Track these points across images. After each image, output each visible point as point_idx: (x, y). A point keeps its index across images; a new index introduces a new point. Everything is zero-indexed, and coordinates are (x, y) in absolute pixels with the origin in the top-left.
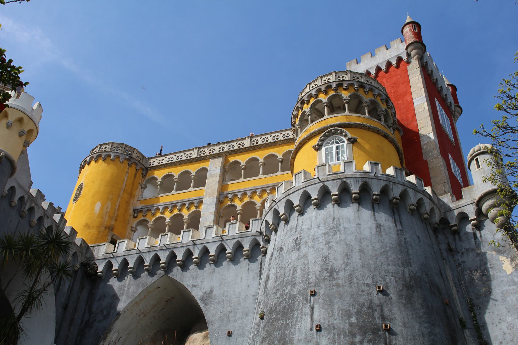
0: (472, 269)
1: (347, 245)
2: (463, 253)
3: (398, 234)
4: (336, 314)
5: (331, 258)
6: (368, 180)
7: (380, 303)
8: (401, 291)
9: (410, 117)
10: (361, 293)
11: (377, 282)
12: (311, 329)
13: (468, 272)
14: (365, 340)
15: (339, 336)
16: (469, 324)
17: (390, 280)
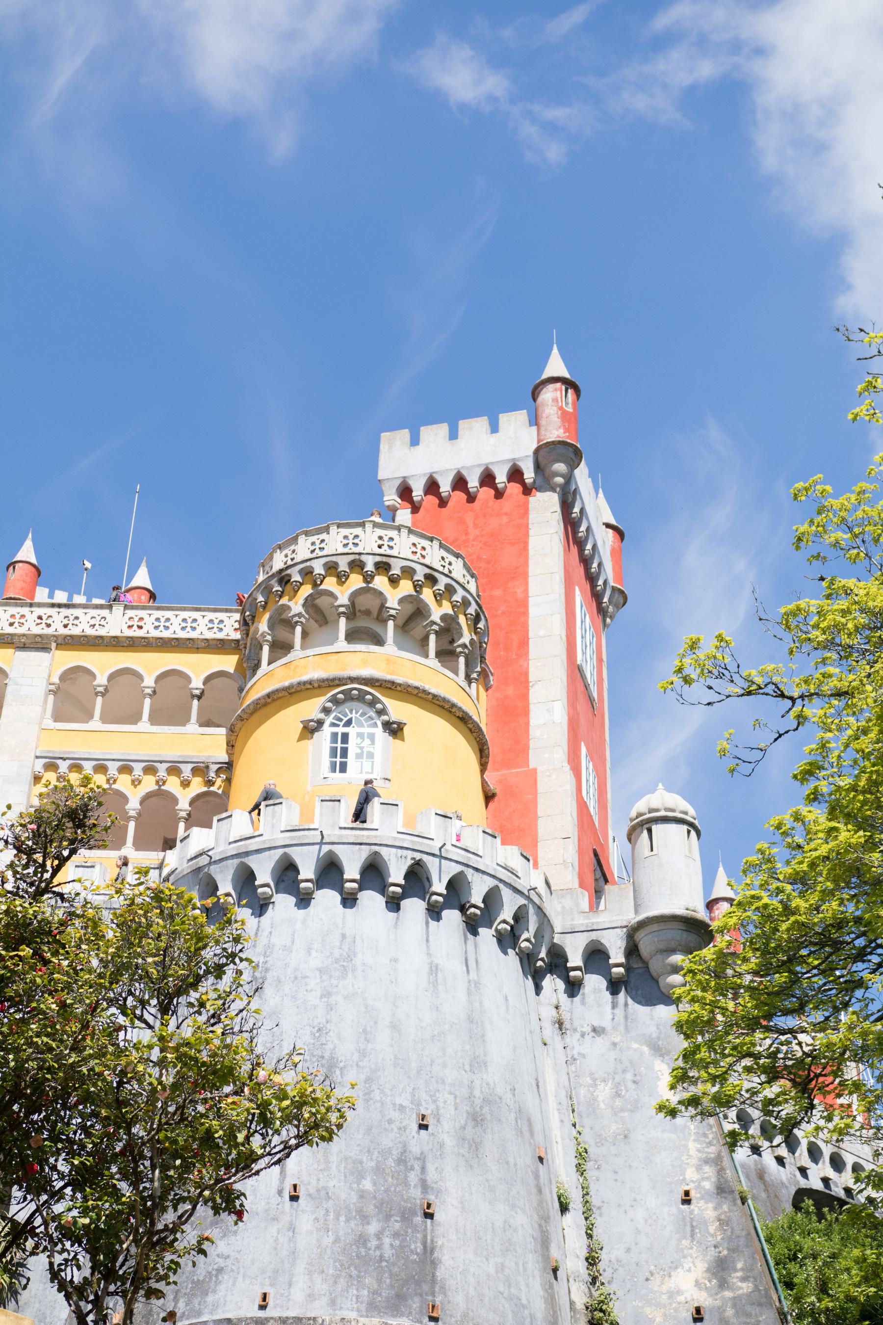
0: (597, 1076)
1: (366, 1006)
2: (583, 1035)
3: (469, 992)
4: (334, 1166)
5: (331, 1033)
6: (425, 858)
7: (422, 1154)
8: (464, 1128)
9: (515, 643)
10: (387, 1126)
11: (419, 1104)
12: (280, 1192)
13: (589, 1081)
14: (387, 1233)
15: (337, 1218)
16: (576, 1205)
17: (445, 1102)
